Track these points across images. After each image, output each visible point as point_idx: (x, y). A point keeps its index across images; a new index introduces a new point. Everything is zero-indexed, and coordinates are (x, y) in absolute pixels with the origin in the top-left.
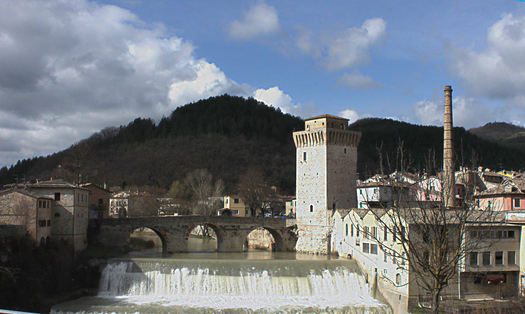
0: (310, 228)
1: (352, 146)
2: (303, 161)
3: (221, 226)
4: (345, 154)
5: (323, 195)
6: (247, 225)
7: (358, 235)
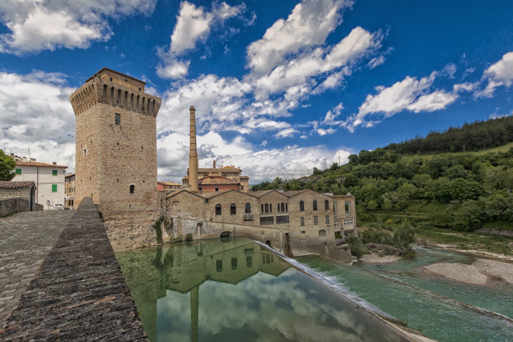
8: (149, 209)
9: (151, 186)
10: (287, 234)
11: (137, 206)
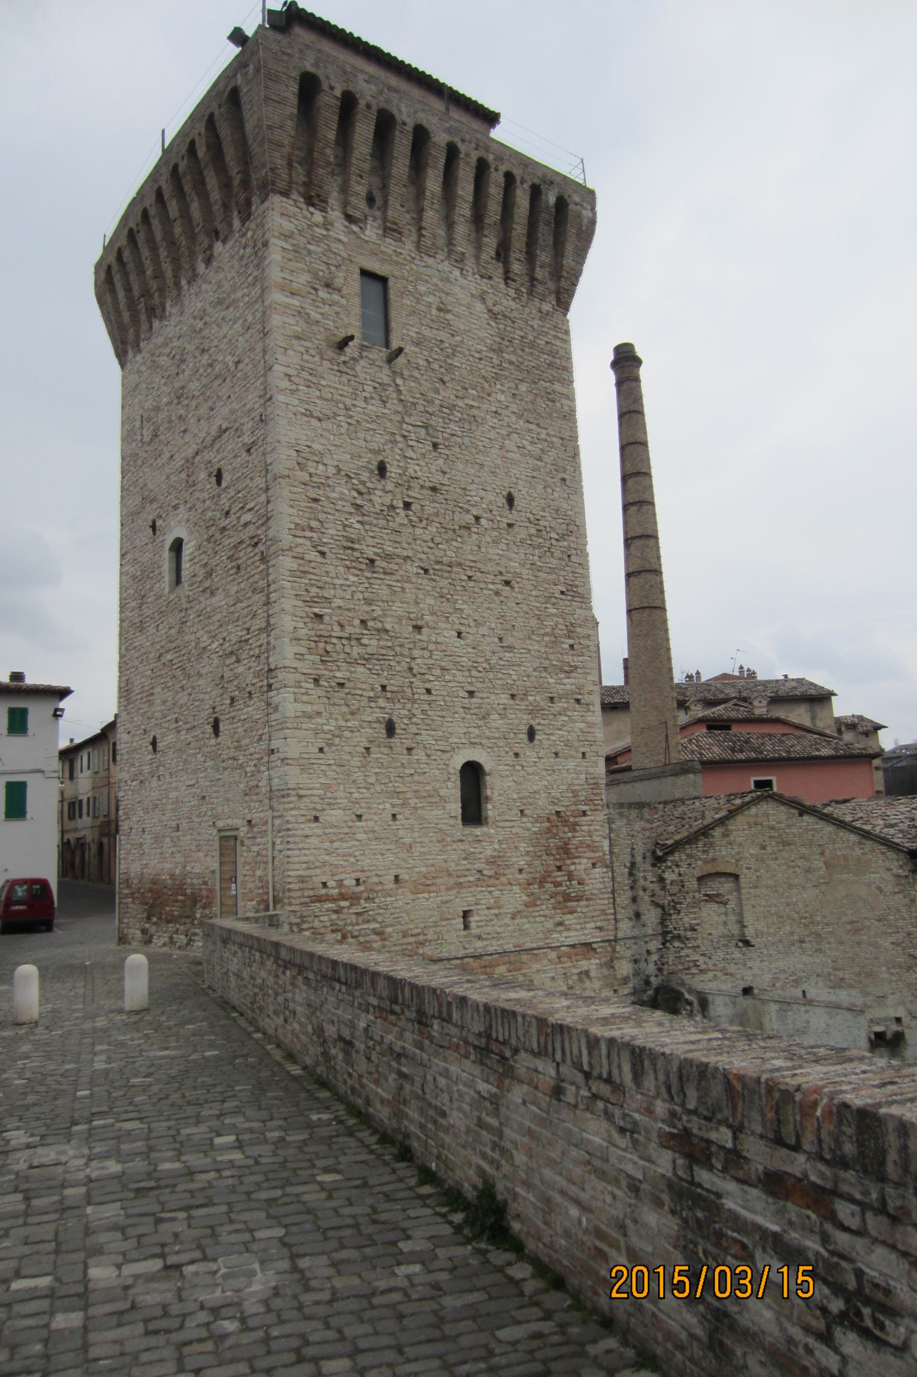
5: (569, 684)
8: (574, 937)
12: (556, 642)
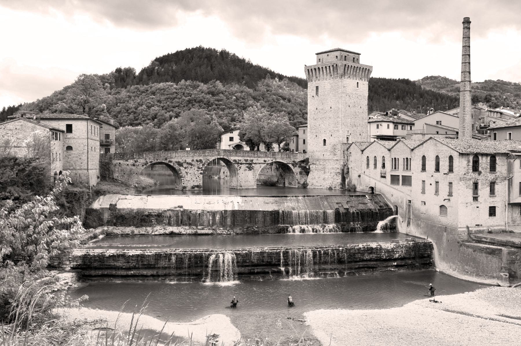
0: (322, 161)
1: (363, 80)
2: (315, 95)
3: (235, 161)
4: (357, 88)
5: (337, 129)
6: (259, 159)
7: (384, 166)
9: (337, 140)
10: (410, 201)
11: (328, 155)
12: (336, 124)
